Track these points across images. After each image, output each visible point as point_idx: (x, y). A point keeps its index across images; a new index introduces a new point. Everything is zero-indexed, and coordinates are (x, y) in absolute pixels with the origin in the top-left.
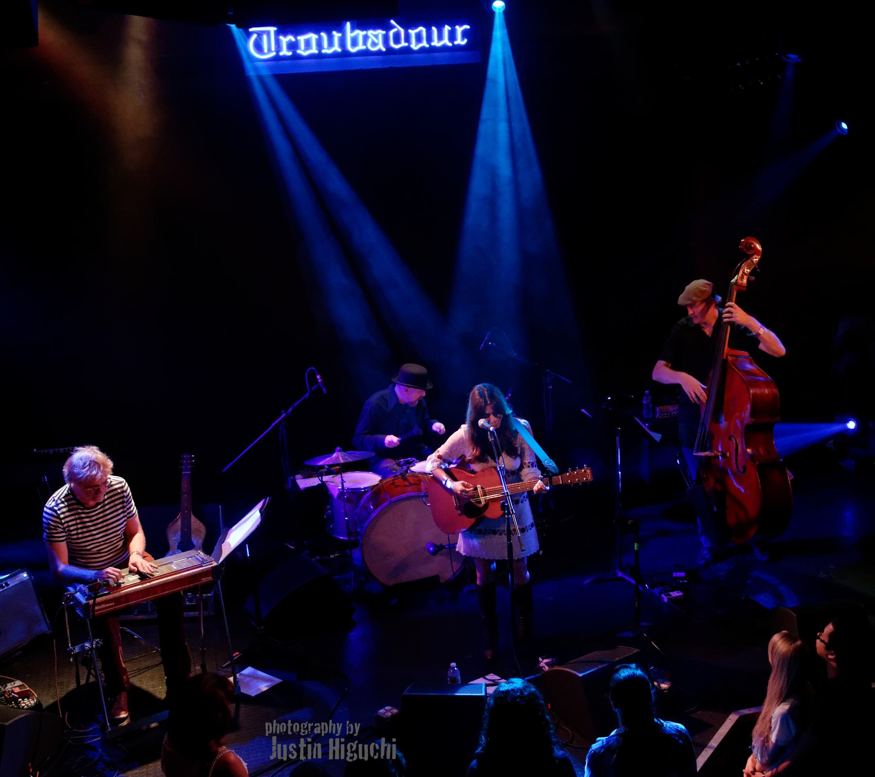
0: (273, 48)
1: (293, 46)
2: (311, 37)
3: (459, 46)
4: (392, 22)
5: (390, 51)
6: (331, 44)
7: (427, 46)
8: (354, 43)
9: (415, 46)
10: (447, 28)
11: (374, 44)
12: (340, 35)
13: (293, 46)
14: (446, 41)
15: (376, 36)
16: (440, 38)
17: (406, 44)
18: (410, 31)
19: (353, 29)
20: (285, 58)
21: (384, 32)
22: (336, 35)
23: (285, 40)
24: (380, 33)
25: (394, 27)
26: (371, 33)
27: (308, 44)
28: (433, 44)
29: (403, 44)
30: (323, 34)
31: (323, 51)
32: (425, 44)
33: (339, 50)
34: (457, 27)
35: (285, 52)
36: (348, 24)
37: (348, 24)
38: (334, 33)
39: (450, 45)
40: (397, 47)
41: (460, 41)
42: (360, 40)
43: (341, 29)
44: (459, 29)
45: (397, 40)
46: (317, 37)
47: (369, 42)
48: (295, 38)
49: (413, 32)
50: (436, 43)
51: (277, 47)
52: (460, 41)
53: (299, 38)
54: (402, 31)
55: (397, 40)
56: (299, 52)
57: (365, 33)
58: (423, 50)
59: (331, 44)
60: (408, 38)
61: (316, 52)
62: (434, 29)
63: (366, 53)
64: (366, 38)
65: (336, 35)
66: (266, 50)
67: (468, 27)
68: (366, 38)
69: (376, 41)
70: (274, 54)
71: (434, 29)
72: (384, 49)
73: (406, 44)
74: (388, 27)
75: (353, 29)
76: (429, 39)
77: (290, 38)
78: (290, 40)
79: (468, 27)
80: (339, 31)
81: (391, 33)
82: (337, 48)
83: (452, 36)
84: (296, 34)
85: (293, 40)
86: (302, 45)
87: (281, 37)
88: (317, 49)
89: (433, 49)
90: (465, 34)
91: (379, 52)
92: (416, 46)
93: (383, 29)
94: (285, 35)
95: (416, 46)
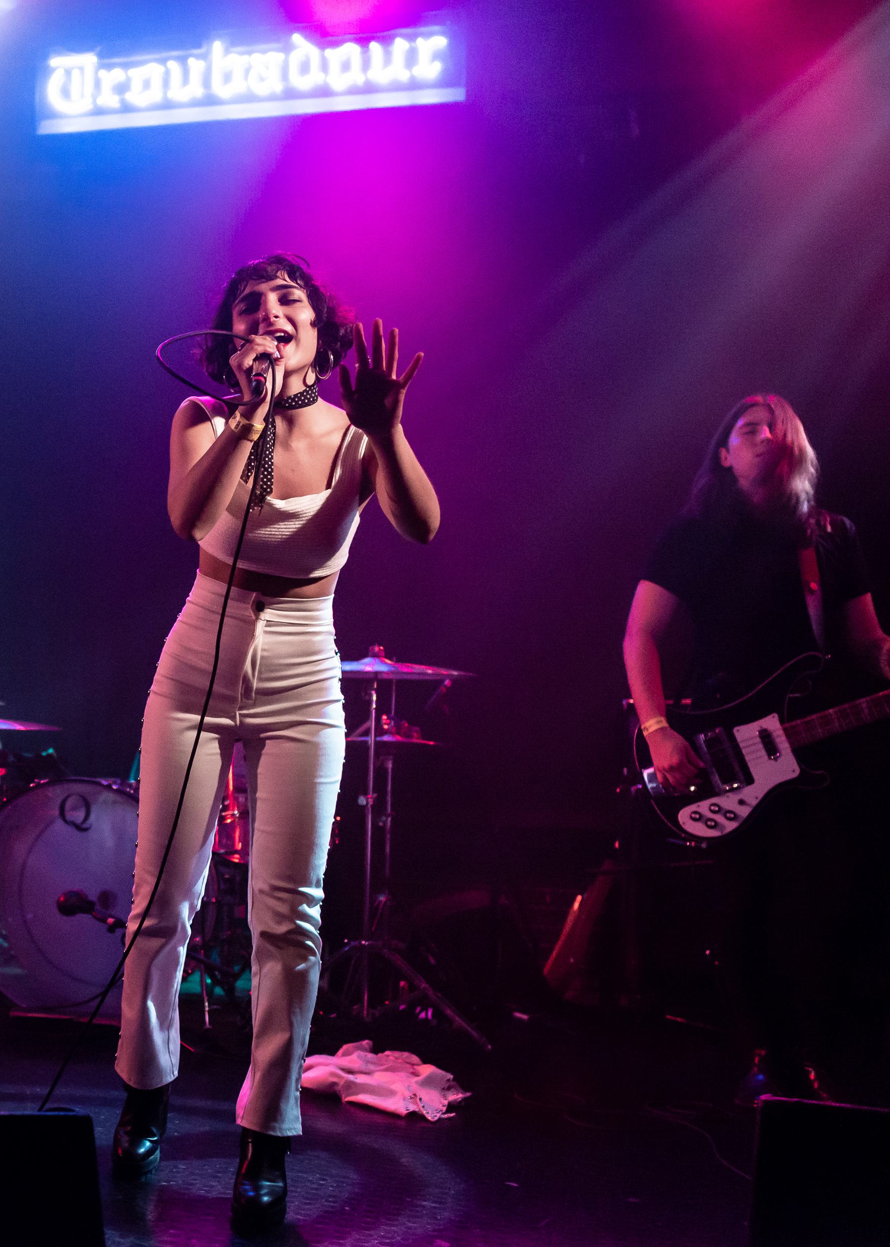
1: (121, 89)
5: (290, 94)
8: (227, 77)
9: (338, 81)
11: (262, 79)
13: (121, 89)
14: (398, 72)
18: (329, 52)
19: (227, 52)
21: (281, 56)
22: (196, 65)
27: (147, 84)
30: (174, 66)
32: (356, 77)
34: (420, 41)
35: (110, 100)
36: (217, 46)
38: (191, 61)
39: (404, 76)
42: (238, 75)
43: (205, 57)
45: (305, 68)
47: (253, 74)
50: (380, 74)
53: (134, 72)
57: (246, 58)
58: (354, 91)
60: (324, 66)
63: (249, 98)
64: (247, 71)
68: (247, 71)
72: (278, 87)
74: (288, 49)
76: (366, 65)
77: (117, 75)
80: (197, 57)
81: (295, 58)
82: (196, 90)
83: (411, 58)
84: (126, 66)
86: (136, 85)
87: (103, 73)
90: (436, 56)
91: (272, 98)
94: (109, 67)
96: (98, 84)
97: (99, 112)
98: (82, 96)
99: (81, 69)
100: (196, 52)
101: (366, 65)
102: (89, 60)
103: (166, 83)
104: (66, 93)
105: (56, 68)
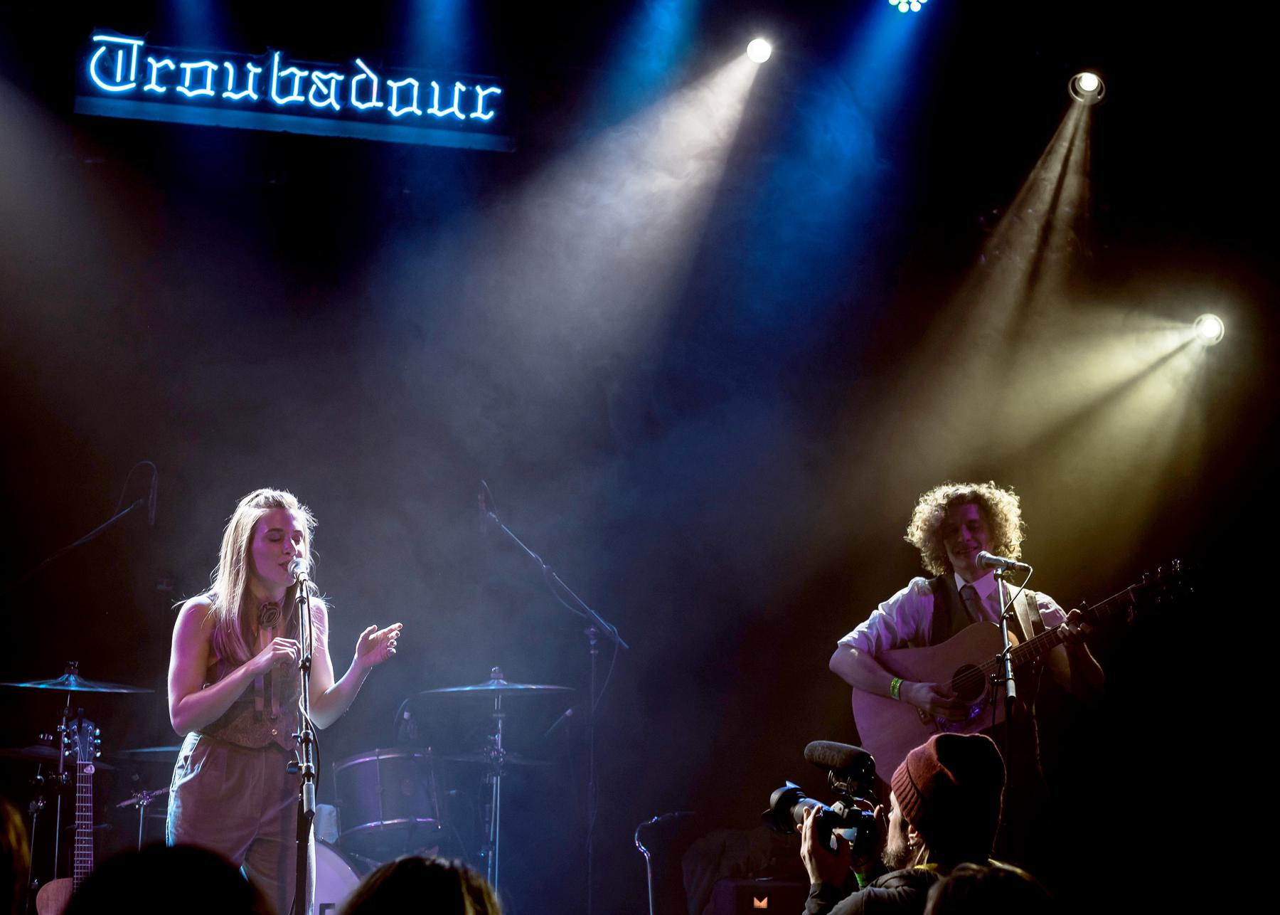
0: (132, 77)
1: (171, 78)
2: (206, 68)
3: (477, 120)
4: (359, 62)
5: (348, 114)
6: (241, 84)
7: (419, 113)
8: (285, 87)
9: (393, 110)
10: (459, 87)
11: (320, 96)
12: (259, 70)
13: (171, 78)
15: (327, 83)
16: (445, 103)
17: (381, 104)
18: (390, 83)
20: (152, 97)
21: (341, 78)
22: (253, 70)
23: (155, 65)
24: (336, 77)
25: (361, 71)
26: (316, 75)
28: (430, 111)
29: (375, 103)
30: (228, 65)
31: (225, 95)
32: (414, 109)
33: (255, 97)
34: (478, 88)
35: (153, 86)
36: (277, 57)
37: (277, 57)
38: (249, 66)
39: (462, 117)
40: (362, 106)
41: (481, 114)
44: (481, 93)
45: (364, 94)
46: (215, 67)
47: (314, 88)
48: (177, 64)
49: (394, 85)
50: (434, 110)
51: (142, 75)
52: (481, 114)
53: (183, 65)
54: (375, 79)
55: (364, 94)
56: (179, 89)
57: (306, 73)
58: (408, 120)
59: (241, 84)
60: (384, 94)
61: (212, 93)
62: (434, 84)
64: (306, 84)
65: (253, 70)
66: (118, 79)
67: (498, 91)
68: (306, 84)
69: (325, 91)
70: (133, 85)
71: (434, 84)
72: (337, 107)
73: (381, 104)
74: (351, 71)
75: (284, 64)
76: (425, 102)
77: (169, 63)
78: (166, 67)
79: (498, 91)
80: (256, 64)
82: (251, 93)
83: (468, 103)
84: (178, 59)
85: (172, 67)
87: (151, 60)
88: (212, 89)
89: (428, 121)
90: (490, 103)
91: (327, 113)
92: (397, 110)
93: (339, 72)
95: (397, 110)
96: (144, 70)
97: (138, 96)
98: (126, 79)
99: (128, 49)
100: (255, 57)
101: (425, 102)
102: (136, 43)
103: (220, 78)
104: (106, 71)
105: (99, 44)
